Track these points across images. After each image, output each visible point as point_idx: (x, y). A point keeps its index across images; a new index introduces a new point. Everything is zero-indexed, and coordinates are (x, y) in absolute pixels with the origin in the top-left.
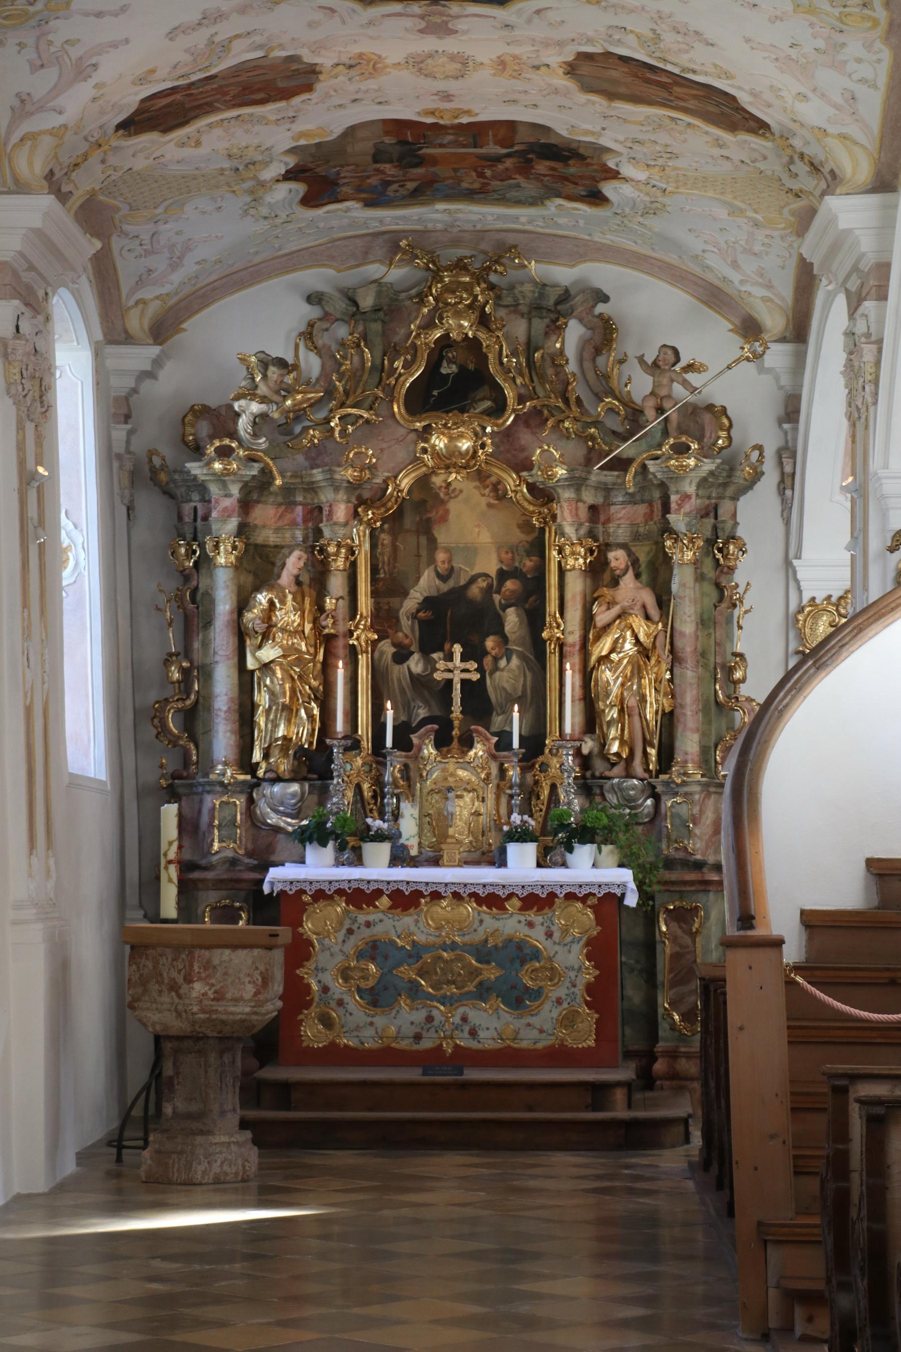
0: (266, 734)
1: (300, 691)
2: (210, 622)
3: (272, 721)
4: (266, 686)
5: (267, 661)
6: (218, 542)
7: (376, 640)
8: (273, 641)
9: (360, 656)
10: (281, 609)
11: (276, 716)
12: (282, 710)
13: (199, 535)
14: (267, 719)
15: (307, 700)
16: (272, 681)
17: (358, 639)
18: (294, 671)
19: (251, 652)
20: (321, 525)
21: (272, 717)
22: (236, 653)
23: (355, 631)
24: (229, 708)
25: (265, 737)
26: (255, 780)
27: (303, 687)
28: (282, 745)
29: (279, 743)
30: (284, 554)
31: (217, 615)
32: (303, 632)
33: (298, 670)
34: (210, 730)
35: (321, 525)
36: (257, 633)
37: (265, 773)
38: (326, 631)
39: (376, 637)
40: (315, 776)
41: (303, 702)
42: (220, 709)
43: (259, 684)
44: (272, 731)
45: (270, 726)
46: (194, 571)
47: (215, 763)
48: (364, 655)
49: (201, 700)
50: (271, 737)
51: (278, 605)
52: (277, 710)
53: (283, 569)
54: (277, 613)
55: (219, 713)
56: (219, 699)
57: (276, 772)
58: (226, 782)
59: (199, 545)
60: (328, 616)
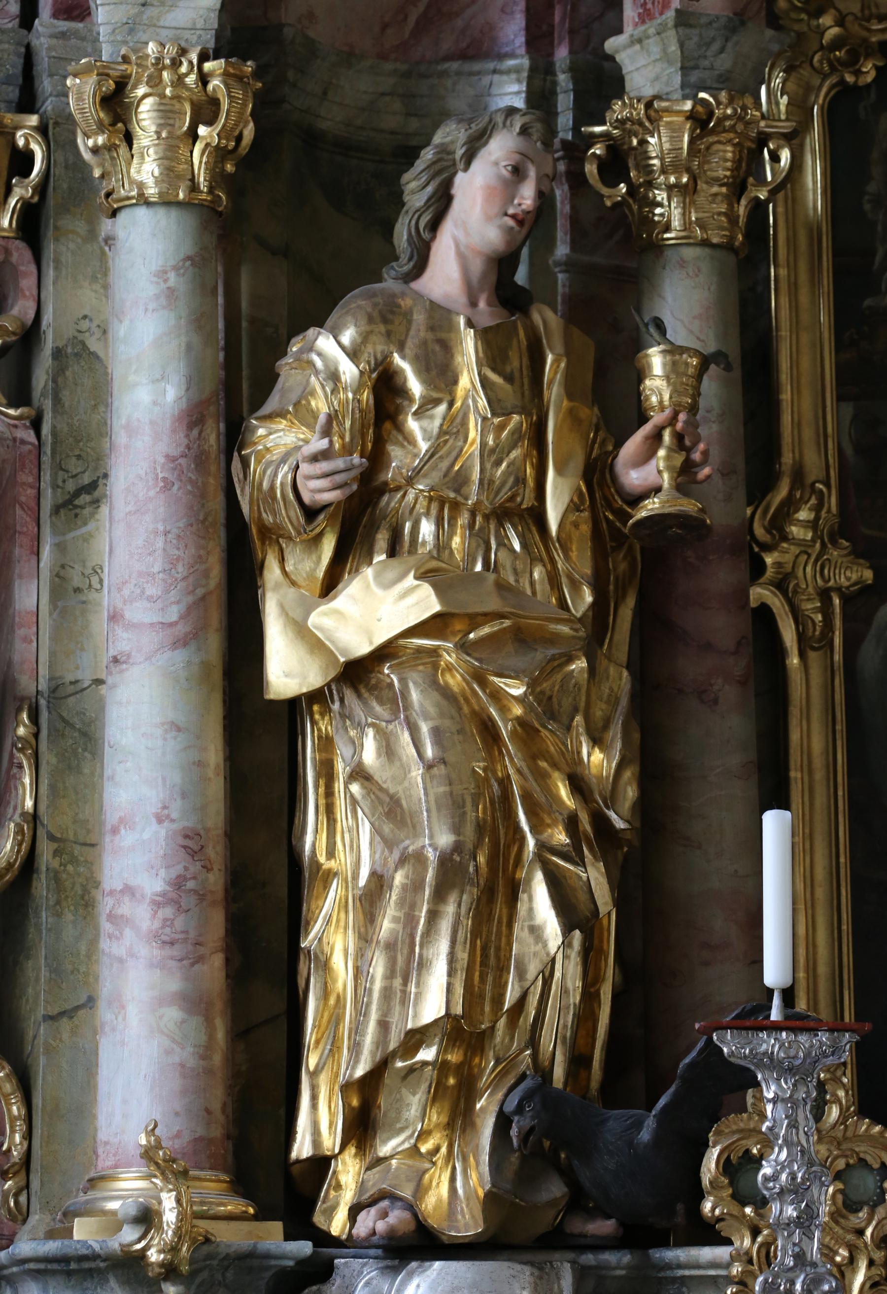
0: (361, 1012)
1: (527, 798)
2: (93, 486)
3: (390, 947)
4: (359, 773)
5: (363, 648)
6: (122, 85)
7: (865, 590)
8: (392, 552)
9: (794, 660)
10: (429, 403)
11: (410, 921)
12: (439, 895)
13: (46, 85)
14: (365, 939)
15: (561, 837)
16: (388, 749)
17: (781, 585)
18: (497, 696)
19: (283, 609)
20: (611, 44)
21: (387, 925)
22: (216, 617)
23: (768, 548)
24: (178, 883)
25: (357, 1029)
26: (305, 1248)
27: (542, 777)
28: (441, 1067)
29: (427, 1054)
30: (445, 151)
31: (120, 437)
32: (538, 516)
33: (517, 690)
34: (91, 1002)
35: (611, 44)
36: (311, 513)
37: (354, 1211)
38: (652, 506)
39: (869, 575)
40: (604, 1227)
41: (541, 846)
42: (129, 890)
43: (327, 772)
44: (387, 994)
45: (378, 968)
46: (21, 253)
47: (104, 1162)
48: (812, 655)
49: (45, 849)
50: (384, 1026)
51: (415, 386)
52: (415, 886)
53: (435, 225)
54: (413, 425)
55: (125, 909)
56: (127, 838)
57: (411, 1208)
58: (154, 1256)
59: (43, 130)
60: (656, 438)
